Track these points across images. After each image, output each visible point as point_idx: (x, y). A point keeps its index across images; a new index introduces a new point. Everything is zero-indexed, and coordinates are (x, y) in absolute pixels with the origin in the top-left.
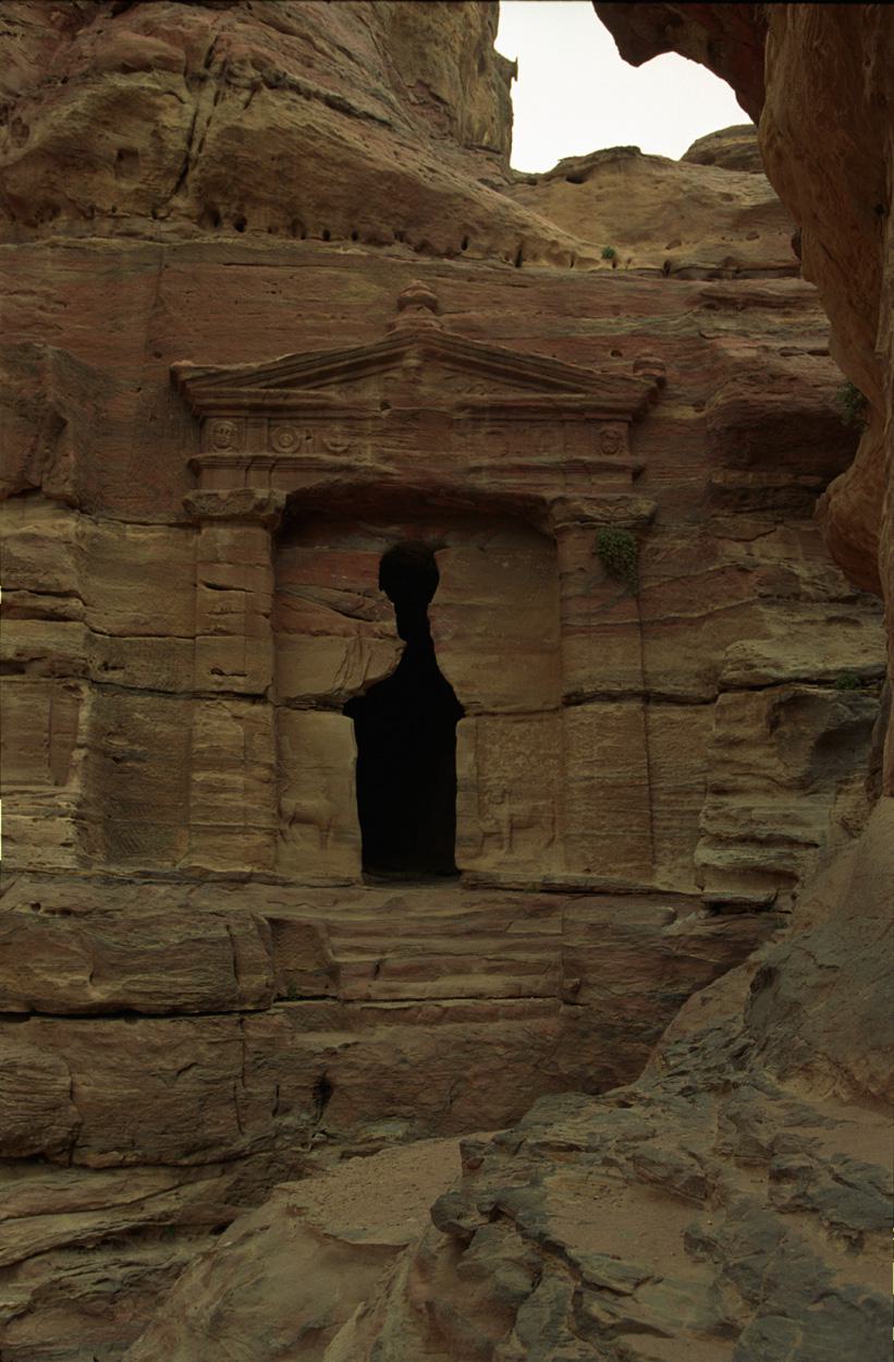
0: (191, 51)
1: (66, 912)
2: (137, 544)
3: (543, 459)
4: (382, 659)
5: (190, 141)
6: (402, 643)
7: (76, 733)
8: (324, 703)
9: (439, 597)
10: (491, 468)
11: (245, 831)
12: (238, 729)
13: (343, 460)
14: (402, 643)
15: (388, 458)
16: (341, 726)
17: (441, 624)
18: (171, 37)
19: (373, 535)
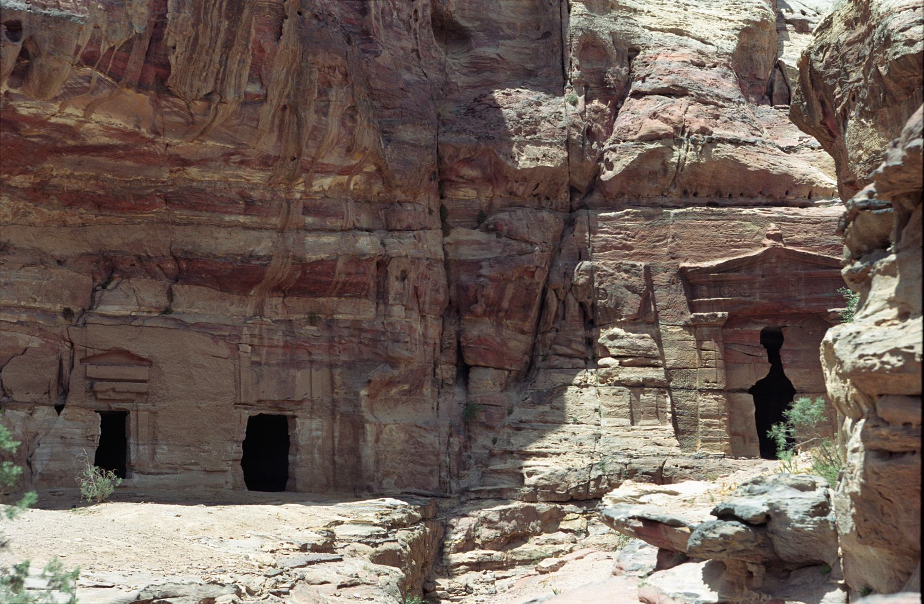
0: (676, 128)
1: (686, 468)
2: (672, 333)
3: (827, 295)
4: (764, 372)
5: (677, 167)
6: (770, 365)
7: (665, 407)
8: (742, 391)
9: (784, 346)
10: (806, 300)
11: (721, 441)
12: (716, 403)
13: (748, 299)
14: (770, 365)
15: (764, 298)
16: (749, 398)
17: (786, 358)
18: (666, 121)
19: (757, 323)
